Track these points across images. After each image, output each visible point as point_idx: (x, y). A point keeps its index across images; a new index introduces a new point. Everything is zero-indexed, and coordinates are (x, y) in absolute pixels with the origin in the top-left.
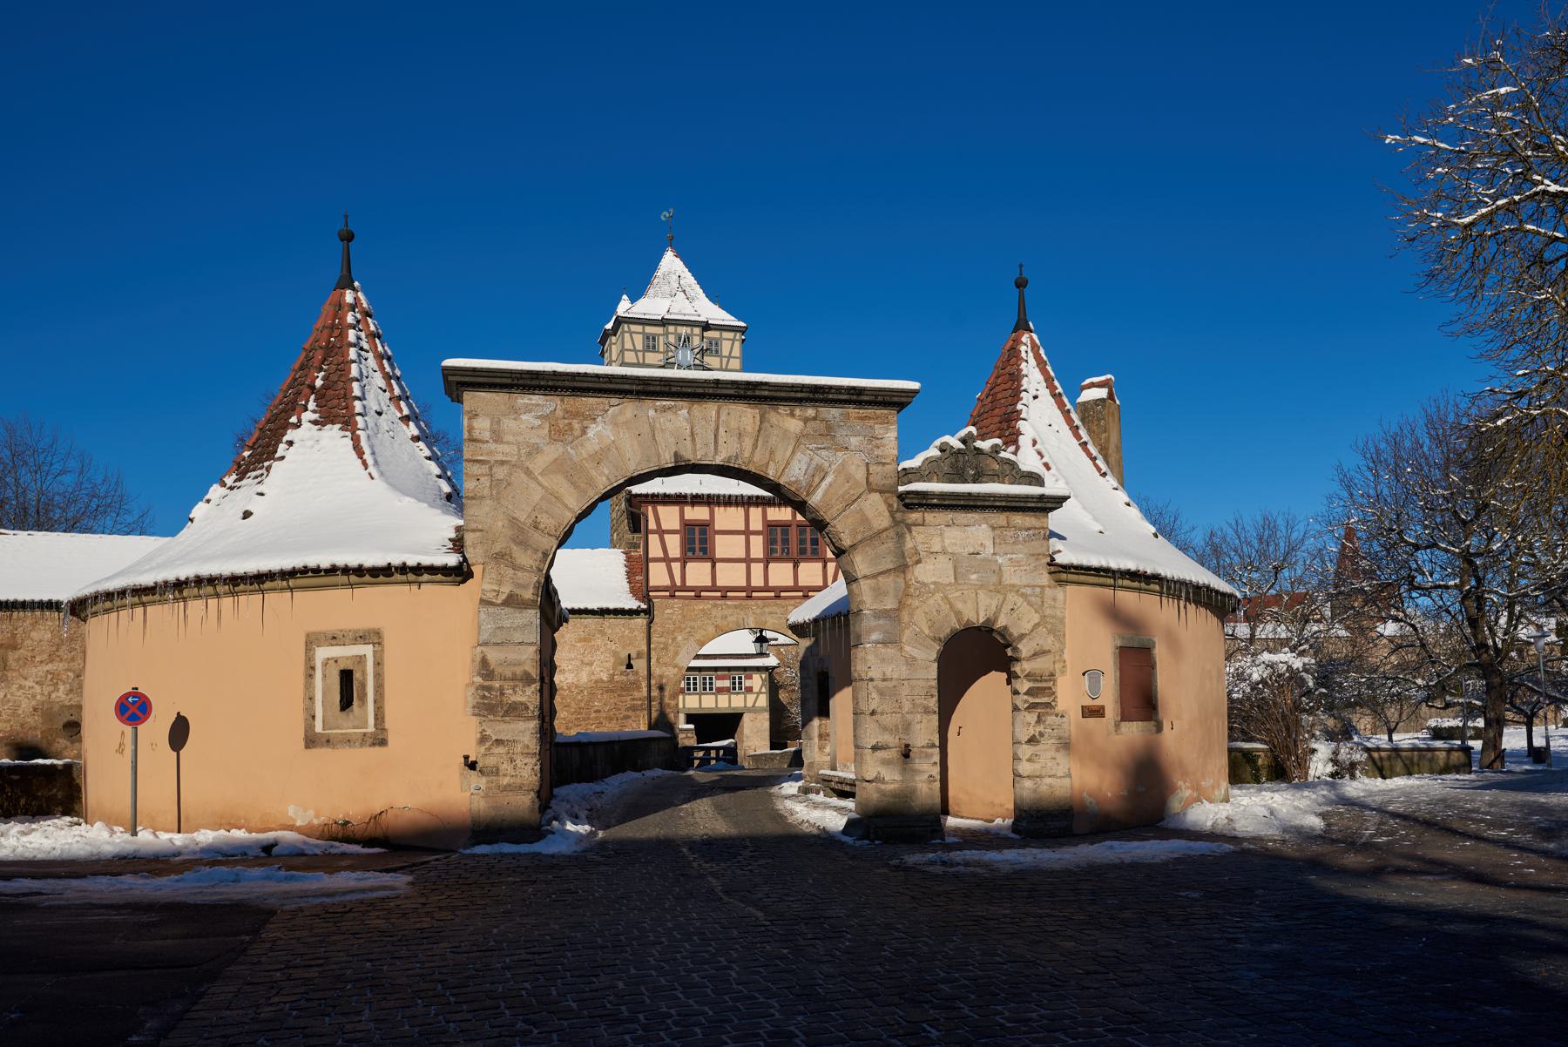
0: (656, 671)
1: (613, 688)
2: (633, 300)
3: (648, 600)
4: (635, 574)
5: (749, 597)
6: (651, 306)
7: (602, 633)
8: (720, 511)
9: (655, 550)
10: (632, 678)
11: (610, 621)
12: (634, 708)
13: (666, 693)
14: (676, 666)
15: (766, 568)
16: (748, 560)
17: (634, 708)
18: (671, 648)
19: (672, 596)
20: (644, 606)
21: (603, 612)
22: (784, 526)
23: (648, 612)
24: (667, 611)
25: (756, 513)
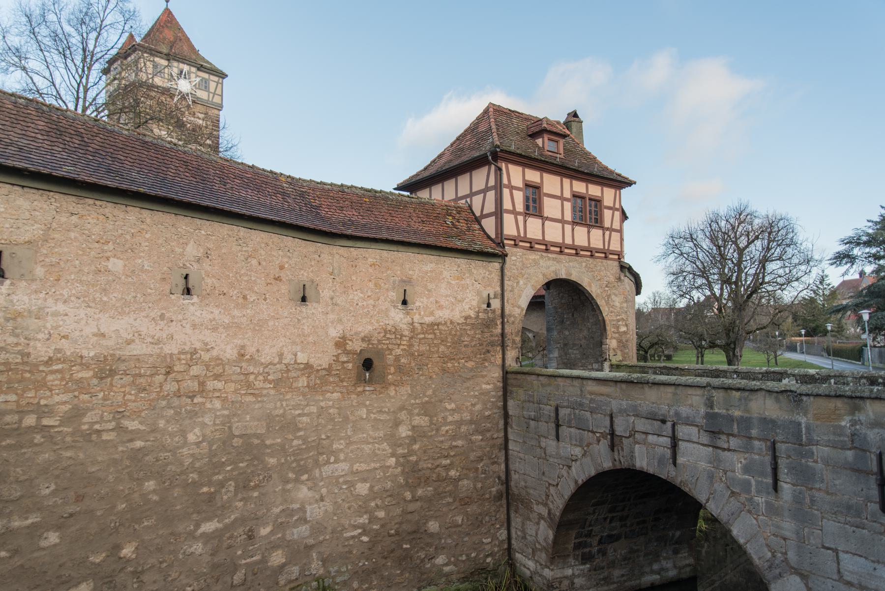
0: (507, 312)
5: (561, 252)
18: (516, 291)
25: (566, 182)
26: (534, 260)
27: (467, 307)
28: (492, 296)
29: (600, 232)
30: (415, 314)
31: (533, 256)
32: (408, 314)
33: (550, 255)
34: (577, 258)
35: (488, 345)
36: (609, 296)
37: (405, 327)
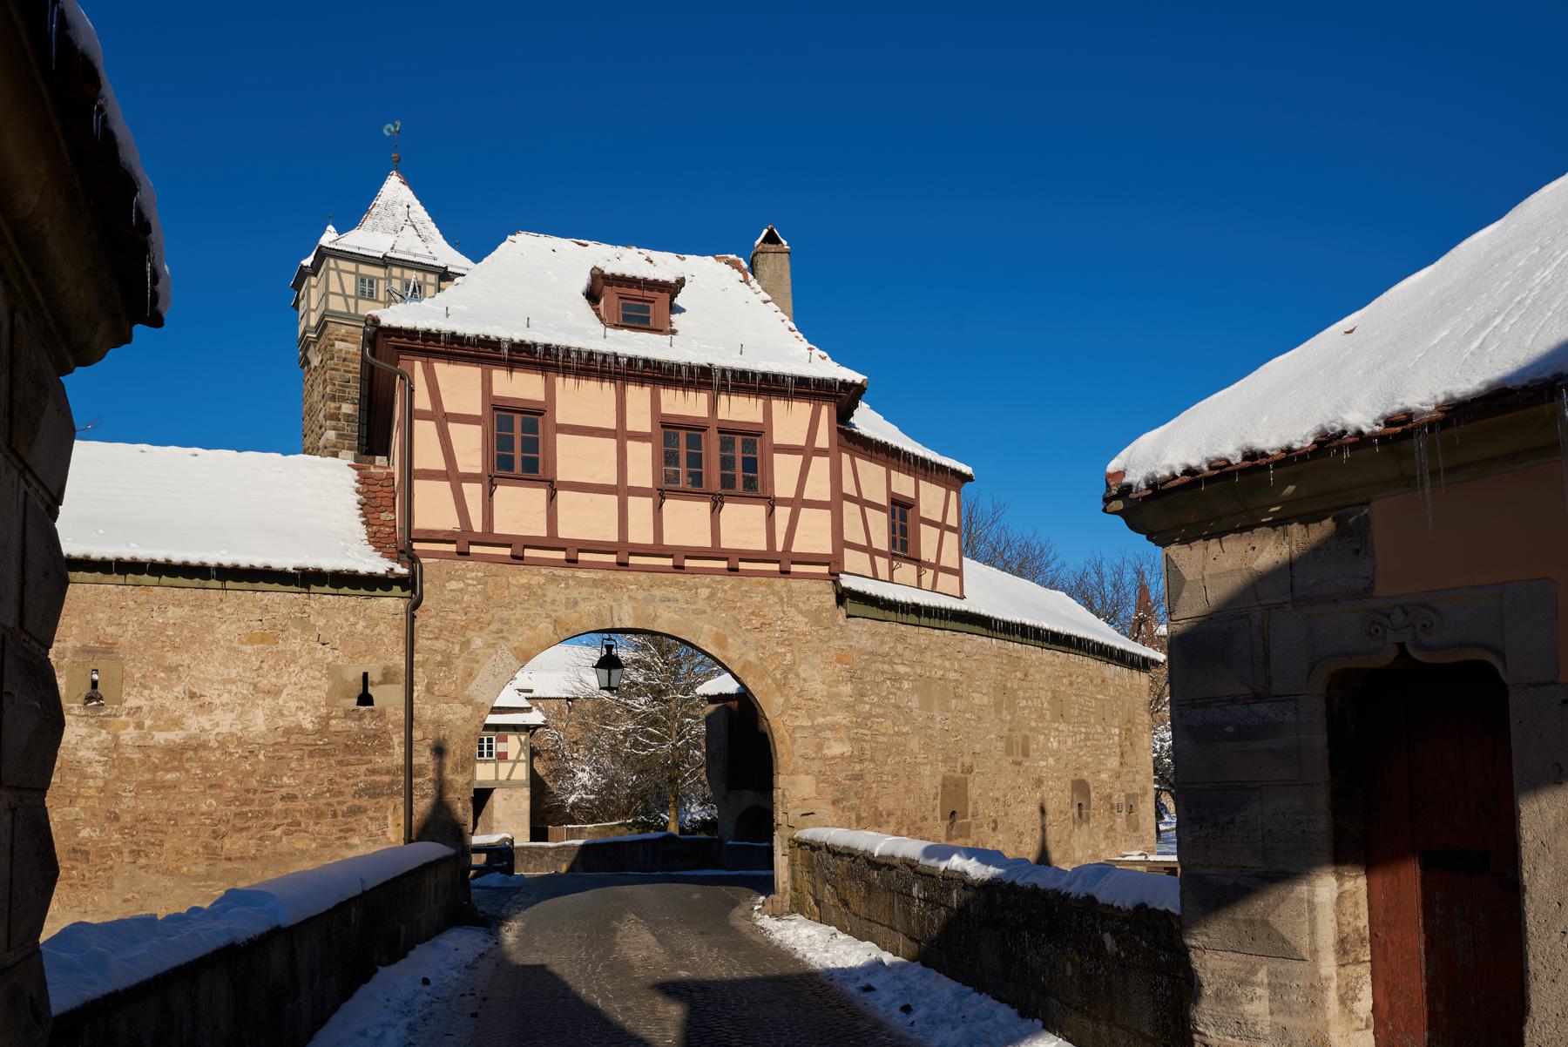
0: (425, 710)
1: (322, 745)
2: (341, 230)
3: (412, 559)
4: (379, 509)
5: (623, 565)
6: (365, 239)
7: (305, 624)
8: (566, 387)
9: (427, 455)
10: (370, 724)
11: (323, 601)
12: (373, 791)
13: (449, 763)
14: (468, 702)
15: (658, 508)
16: (622, 490)
17: (373, 791)
18: (459, 664)
19: (463, 554)
20: (401, 570)
21: (307, 579)
22: (694, 429)
23: (410, 583)
24: (451, 586)
25: (638, 396)
26: (528, 587)
27: (293, 705)
28: (374, 676)
29: (760, 510)
30: (126, 725)
31: (521, 577)
32: (103, 725)
33: (582, 574)
34: (680, 577)
35: (358, 794)
36: (789, 670)
37: (93, 755)
